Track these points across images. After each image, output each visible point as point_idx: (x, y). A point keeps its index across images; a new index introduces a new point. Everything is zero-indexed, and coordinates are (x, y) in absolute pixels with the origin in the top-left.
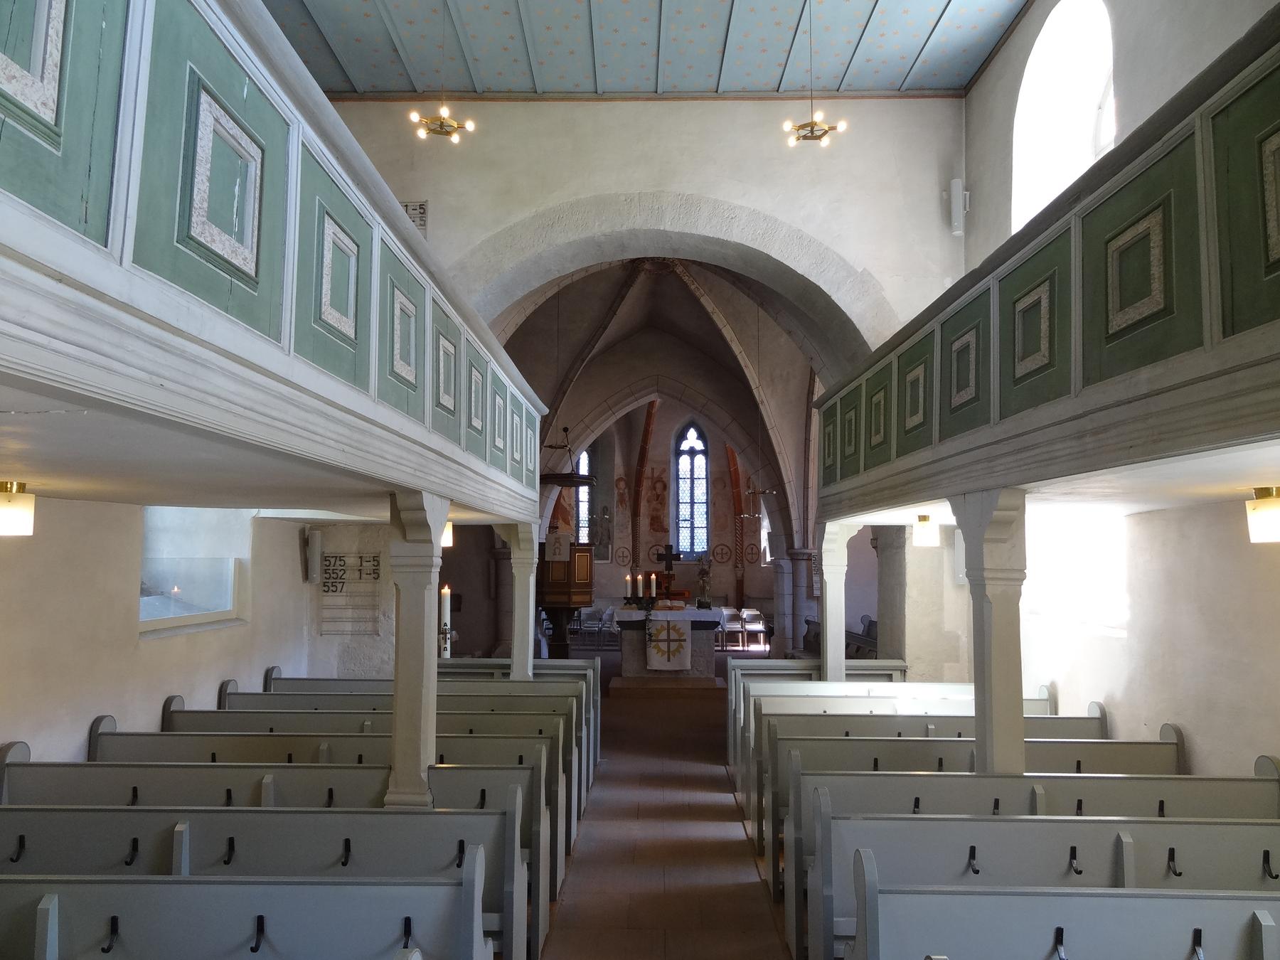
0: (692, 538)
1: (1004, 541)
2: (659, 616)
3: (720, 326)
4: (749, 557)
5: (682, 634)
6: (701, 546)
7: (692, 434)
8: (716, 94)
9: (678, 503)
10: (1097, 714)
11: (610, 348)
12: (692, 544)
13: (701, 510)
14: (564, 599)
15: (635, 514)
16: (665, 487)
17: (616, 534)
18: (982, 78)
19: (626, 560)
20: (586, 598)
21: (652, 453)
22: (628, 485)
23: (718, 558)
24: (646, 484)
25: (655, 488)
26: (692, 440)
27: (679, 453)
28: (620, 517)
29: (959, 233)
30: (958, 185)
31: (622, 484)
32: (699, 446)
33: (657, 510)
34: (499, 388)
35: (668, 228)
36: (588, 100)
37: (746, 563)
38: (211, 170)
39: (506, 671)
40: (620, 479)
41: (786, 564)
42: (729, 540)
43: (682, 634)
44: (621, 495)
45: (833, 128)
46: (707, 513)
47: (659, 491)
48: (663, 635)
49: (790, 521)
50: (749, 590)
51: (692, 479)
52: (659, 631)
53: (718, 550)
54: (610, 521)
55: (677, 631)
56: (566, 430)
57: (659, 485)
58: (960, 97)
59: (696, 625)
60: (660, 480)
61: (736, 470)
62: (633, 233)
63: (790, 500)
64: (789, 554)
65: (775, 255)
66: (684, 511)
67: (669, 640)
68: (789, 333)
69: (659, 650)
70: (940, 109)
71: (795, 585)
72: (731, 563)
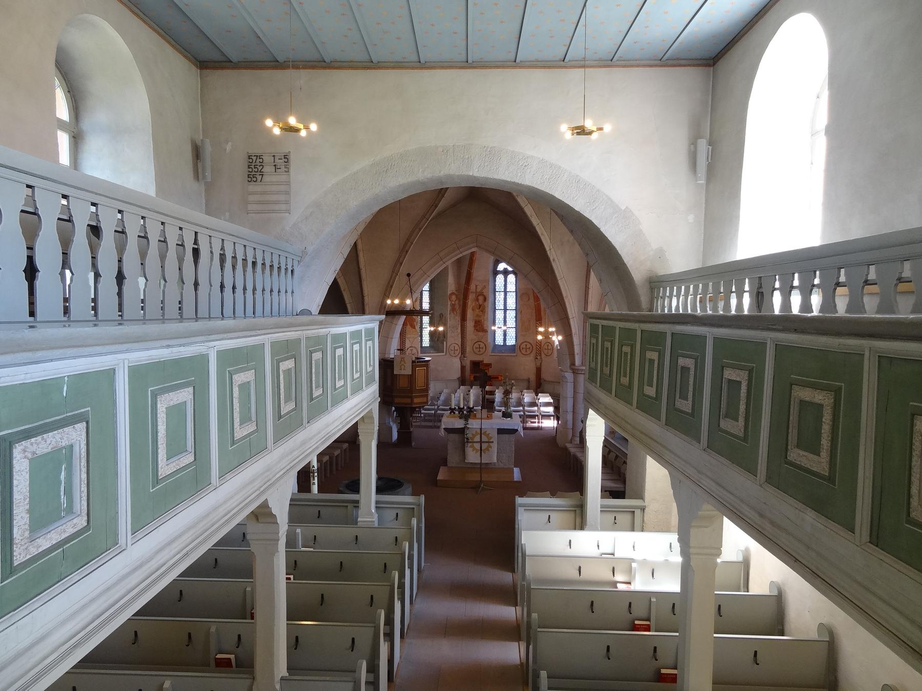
1: (706, 527)
2: (474, 424)
3: (523, 205)
4: (546, 352)
5: (491, 438)
6: (511, 341)
8: (515, 63)
9: (495, 309)
10: (775, 593)
11: (440, 215)
12: (505, 340)
13: (511, 315)
14: (409, 400)
15: (463, 319)
16: (485, 299)
18: (727, 55)
19: (457, 353)
20: (424, 400)
23: (524, 351)
24: (471, 297)
25: (477, 300)
27: (496, 273)
29: (702, 182)
30: (703, 144)
31: (454, 297)
34: (339, 340)
35: (476, 174)
36: (413, 68)
37: (543, 356)
38: (30, 503)
39: (353, 521)
40: (453, 294)
41: (569, 376)
43: (491, 438)
44: (453, 306)
45: (600, 129)
46: (516, 317)
48: (477, 439)
49: (573, 345)
50: (544, 376)
51: (505, 292)
52: (474, 436)
53: (523, 346)
55: (488, 435)
56: (409, 275)
57: (481, 298)
58: (709, 66)
59: (501, 431)
60: (481, 294)
62: (450, 177)
63: (573, 331)
64: (572, 369)
65: (558, 195)
66: (499, 315)
67: (481, 442)
68: (572, 232)
69: (474, 449)
70: (691, 76)
71: (575, 392)
72: (532, 355)
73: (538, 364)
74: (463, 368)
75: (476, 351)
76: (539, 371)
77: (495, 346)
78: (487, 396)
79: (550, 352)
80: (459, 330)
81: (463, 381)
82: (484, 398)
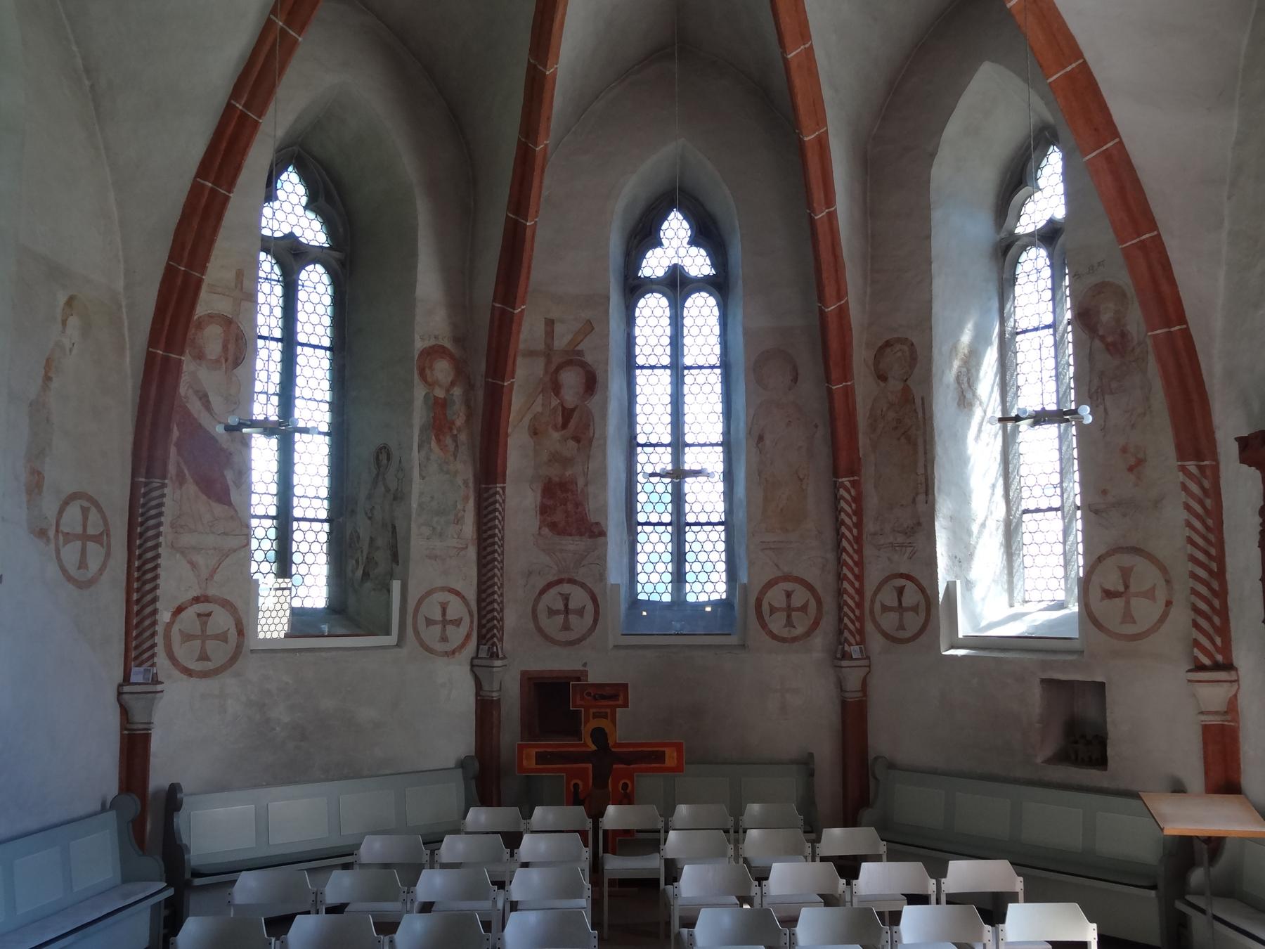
0: (679, 557)
6: (709, 584)
7: (676, 228)
12: (679, 577)
16: (591, 383)
17: (418, 544)
19: (456, 635)
22: (461, 372)
25: (556, 388)
26: (676, 247)
27: (635, 288)
28: (435, 484)
31: (442, 370)
32: (698, 264)
33: (566, 462)
37: (876, 643)
42: (812, 562)
44: (439, 407)
47: (570, 395)
51: (677, 368)
53: (776, 596)
54: (399, 497)
57: (571, 380)
60: (573, 359)
61: (843, 312)
72: (819, 641)
73: (853, 681)
74: (486, 709)
75: (552, 625)
76: (853, 716)
77: (635, 604)
78: (616, 865)
79: (913, 622)
81: (486, 779)
82: (596, 867)
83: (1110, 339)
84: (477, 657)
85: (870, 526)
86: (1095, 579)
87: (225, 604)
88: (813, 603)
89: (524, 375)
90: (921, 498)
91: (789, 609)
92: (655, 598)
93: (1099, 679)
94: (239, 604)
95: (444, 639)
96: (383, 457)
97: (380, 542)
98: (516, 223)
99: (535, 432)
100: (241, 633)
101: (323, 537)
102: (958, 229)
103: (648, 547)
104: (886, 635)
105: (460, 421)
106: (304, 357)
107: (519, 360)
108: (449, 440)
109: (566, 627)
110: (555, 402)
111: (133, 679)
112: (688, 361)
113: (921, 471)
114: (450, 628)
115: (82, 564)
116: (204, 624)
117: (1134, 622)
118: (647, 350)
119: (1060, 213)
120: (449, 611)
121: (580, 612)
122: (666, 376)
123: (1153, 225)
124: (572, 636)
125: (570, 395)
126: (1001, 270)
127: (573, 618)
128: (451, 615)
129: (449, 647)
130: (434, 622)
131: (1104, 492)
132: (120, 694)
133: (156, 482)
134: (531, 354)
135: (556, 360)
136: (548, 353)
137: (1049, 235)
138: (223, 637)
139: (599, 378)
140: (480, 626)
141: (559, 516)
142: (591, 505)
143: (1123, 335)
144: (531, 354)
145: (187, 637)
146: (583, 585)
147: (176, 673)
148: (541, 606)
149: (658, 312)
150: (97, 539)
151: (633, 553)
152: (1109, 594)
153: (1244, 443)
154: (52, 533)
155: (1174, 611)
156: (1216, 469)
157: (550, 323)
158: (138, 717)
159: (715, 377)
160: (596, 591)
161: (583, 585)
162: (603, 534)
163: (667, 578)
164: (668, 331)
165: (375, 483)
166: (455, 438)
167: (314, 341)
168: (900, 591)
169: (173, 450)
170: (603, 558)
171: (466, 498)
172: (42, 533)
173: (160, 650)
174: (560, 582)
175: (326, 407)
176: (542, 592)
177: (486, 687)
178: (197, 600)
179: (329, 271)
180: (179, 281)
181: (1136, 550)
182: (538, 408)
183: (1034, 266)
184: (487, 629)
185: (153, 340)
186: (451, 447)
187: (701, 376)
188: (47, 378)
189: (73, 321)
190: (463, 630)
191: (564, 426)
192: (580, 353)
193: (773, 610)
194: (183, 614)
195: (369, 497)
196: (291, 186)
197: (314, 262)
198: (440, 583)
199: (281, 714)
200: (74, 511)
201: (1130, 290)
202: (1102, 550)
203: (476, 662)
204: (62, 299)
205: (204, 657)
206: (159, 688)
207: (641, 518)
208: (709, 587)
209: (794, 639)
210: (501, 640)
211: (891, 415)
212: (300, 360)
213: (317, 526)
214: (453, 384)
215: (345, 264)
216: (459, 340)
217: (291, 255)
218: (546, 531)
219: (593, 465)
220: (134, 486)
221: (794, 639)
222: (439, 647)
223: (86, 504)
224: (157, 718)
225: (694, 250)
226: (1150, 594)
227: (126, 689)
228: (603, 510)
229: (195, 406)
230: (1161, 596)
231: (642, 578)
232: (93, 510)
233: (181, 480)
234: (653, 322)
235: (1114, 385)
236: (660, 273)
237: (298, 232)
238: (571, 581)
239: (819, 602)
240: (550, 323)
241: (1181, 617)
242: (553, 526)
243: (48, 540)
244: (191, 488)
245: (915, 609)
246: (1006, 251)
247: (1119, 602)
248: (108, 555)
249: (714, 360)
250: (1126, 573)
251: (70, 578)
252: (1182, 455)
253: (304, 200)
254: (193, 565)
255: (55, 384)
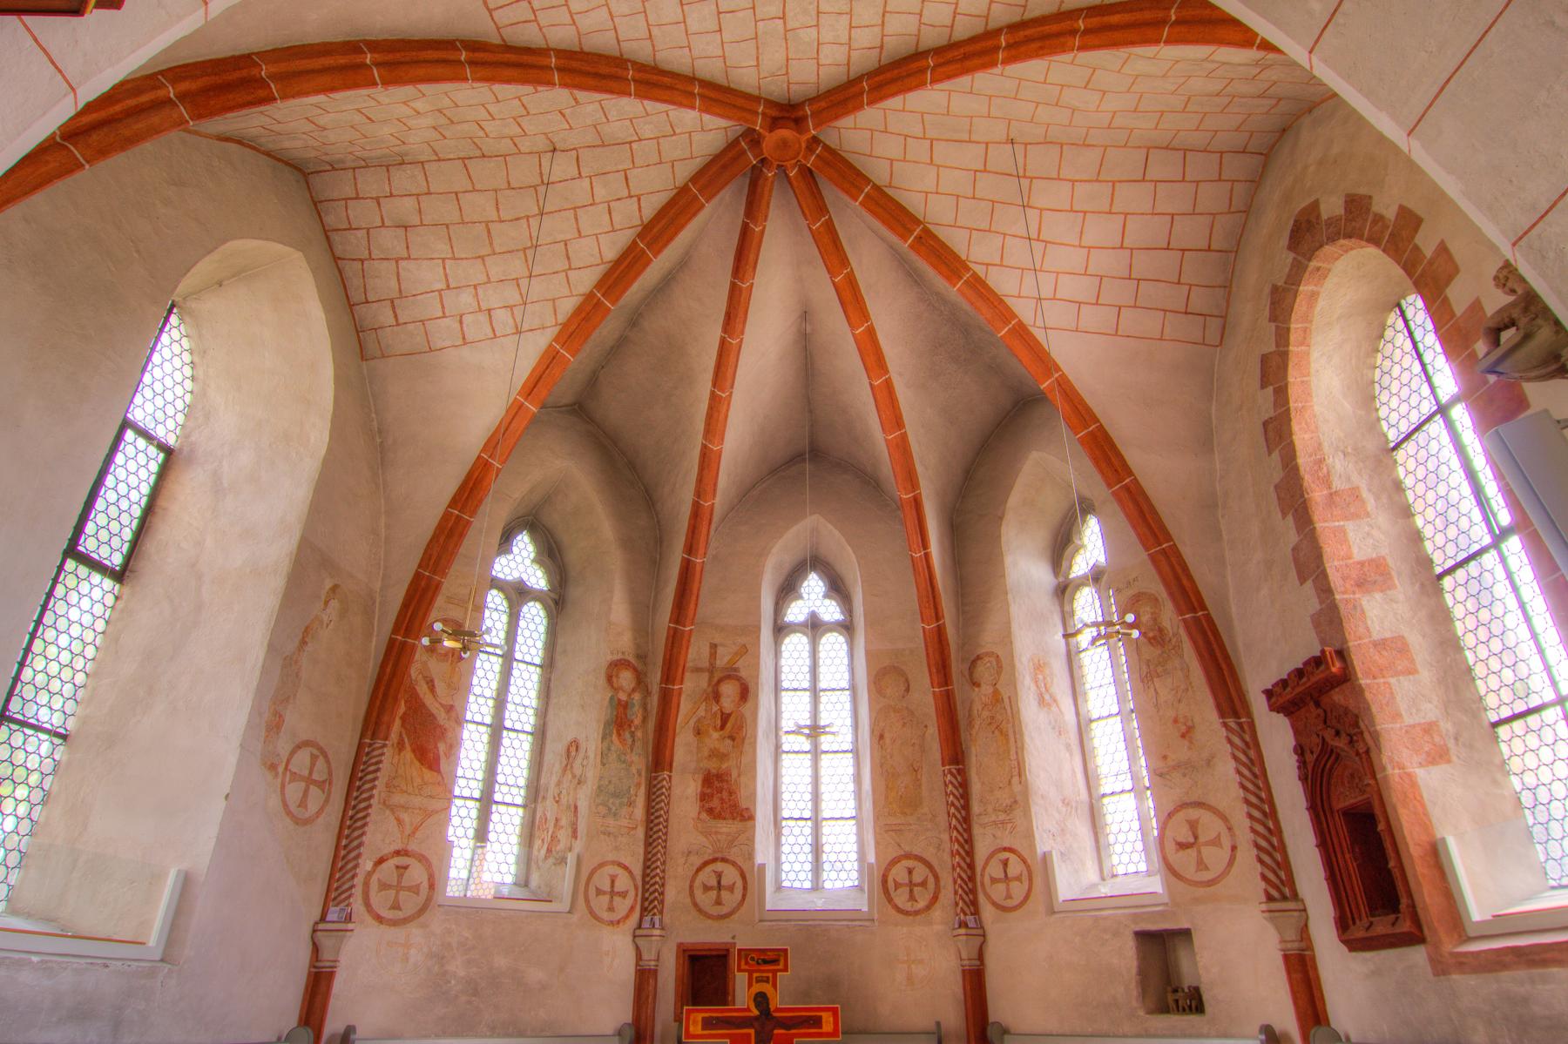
0: (817, 849)
7: (813, 585)
15: (660, 760)
16: (746, 693)
19: (623, 906)
21: (711, 605)
23: (901, 898)
25: (717, 696)
26: (813, 597)
32: (831, 611)
33: (723, 757)
37: (987, 912)
47: (728, 704)
53: (899, 873)
57: (729, 690)
60: (731, 674)
74: (645, 978)
79: (1018, 890)
80: (639, 811)
83: (1151, 635)
84: (640, 927)
85: (976, 808)
86: (1168, 833)
87: (423, 859)
88: (931, 880)
89: (691, 686)
90: (1015, 780)
91: (911, 884)
92: (797, 885)
93: (1185, 926)
94: (434, 861)
95: (611, 909)
96: (573, 749)
97: (564, 822)
98: (688, 561)
99: (698, 732)
100: (432, 886)
101: (517, 821)
102: (1024, 567)
103: (791, 840)
104: (994, 904)
105: (637, 721)
106: (518, 670)
107: (687, 675)
108: (627, 735)
109: (718, 902)
110: (715, 708)
111: (330, 917)
112: (822, 685)
113: (1013, 757)
114: (617, 899)
115: (303, 804)
116: (401, 876)
117: (1207, 868)
118: (791, 677)
119: (1102, 559)
120: (617, 884)
121: (731, 888)
122: (806, 697)
123: (1169, 537)
124: (724, 910)
125: (728, 704)
126: (1062, 605)
127: (725, 894)
128: (619, 887)
129: (616, 916)
130: (604, 893)
131: (1165, 757)
132: (314, 931)
133: (379, 743)
134: (698, 670)
135: (717, 676)
136: (711, 669)
137: (1096, 576)
138: (415, 889)
139: (751, 690)
140: (644, 899)
141: (715, 803)
142: (743, 793)
143: (1161, 630)
144: (698, 670)
145: (384, 886)
146: (734, 864)
147: (369, 919)
148: (697, 883)
149: (800, 647)
150: (320, 785)
151: (778, 844)
152: (1182, 846)
153: (1269, 694)
154: (281, 769)
155: (1239, 853)
156: (1252, 725)
157: (714, 646)
158: (326, 955)
159: (845, 697)
160: (745, 868)
161: (734, 864)
162: (751, 818)
163: (808, 867)
164: (808, 662)
165: (565, 770)
166: (633, 734)
167: (528, 659)
168: (1005, 863)
169: (398, 722)
170: (751, 840)
171: (639, 785)
172: (273, 767)
173: (358, 892)
174: (714, 860)
175: (531, 712)
176: (699, 870)
177: (645, 956)
178: (398, 853)
179: (546, 607)
180: (423, 584)
181: (1199, 804)
182: (701, 712)
183: (1087, 606)
184: (650, 901)
185: (396, 630)
186: (629, 741)
187: (834, 696)
188: (304, 642)
189: (334, 604)
190: (629, 902)
191: (722, 727)
192: (736, 670)
193: (897, 885)
194: (384, 865)
195: (559, 784)
196: (524, 545)
197: (535, 599)
198: (610, 857)
199: (457, 967)
200: (303, 757)
201: (1162, 593)
202: (1171, 807)
203: (639, 932)
204: (328, 584)
205: (396, 906)
206: (350, 926)
207: (785, 814)
208: (843, 875)
209: (917, 913)
210: (661, 912)
211: (986, 714)
212: (515, 672)
213: (513, 810)
214: (634, 690)
215: (558, 603)
216: (642, 657)
217: (518, 594)
218: (704, 815)
219: (745, 760)
220: (360, 746)
221: (917, 913)
222: (605, 915)
223: (315, 752)
224: (344, 960)
225: (827, 602)
226: (1216, 842)
227: (321, 926)
228: (753, 795)
229: (422, 689)
230: (1227, 844)
231: (786, 867)
232: (321, 760)
233: (400, 746)
234: (796, 655)
235: (1160, 669)
236: (801, 618)
237: (525, 577)
238: (724, 860)
239: (936, 877)
240: (714, 646)
241: (1247, 855)
242: (710, 811)
243: (277, 775)
244: (408, 754)
245: (1018, 879)
246: (1064, 591)
247: (1192, 852)
248: (327, 801)
249: (845, 684)
250: (1193, 826)
251: (289, 813)
252: (1222, 715)
253: (532, 555)
254: (399, 821)
255: (309, 648)
